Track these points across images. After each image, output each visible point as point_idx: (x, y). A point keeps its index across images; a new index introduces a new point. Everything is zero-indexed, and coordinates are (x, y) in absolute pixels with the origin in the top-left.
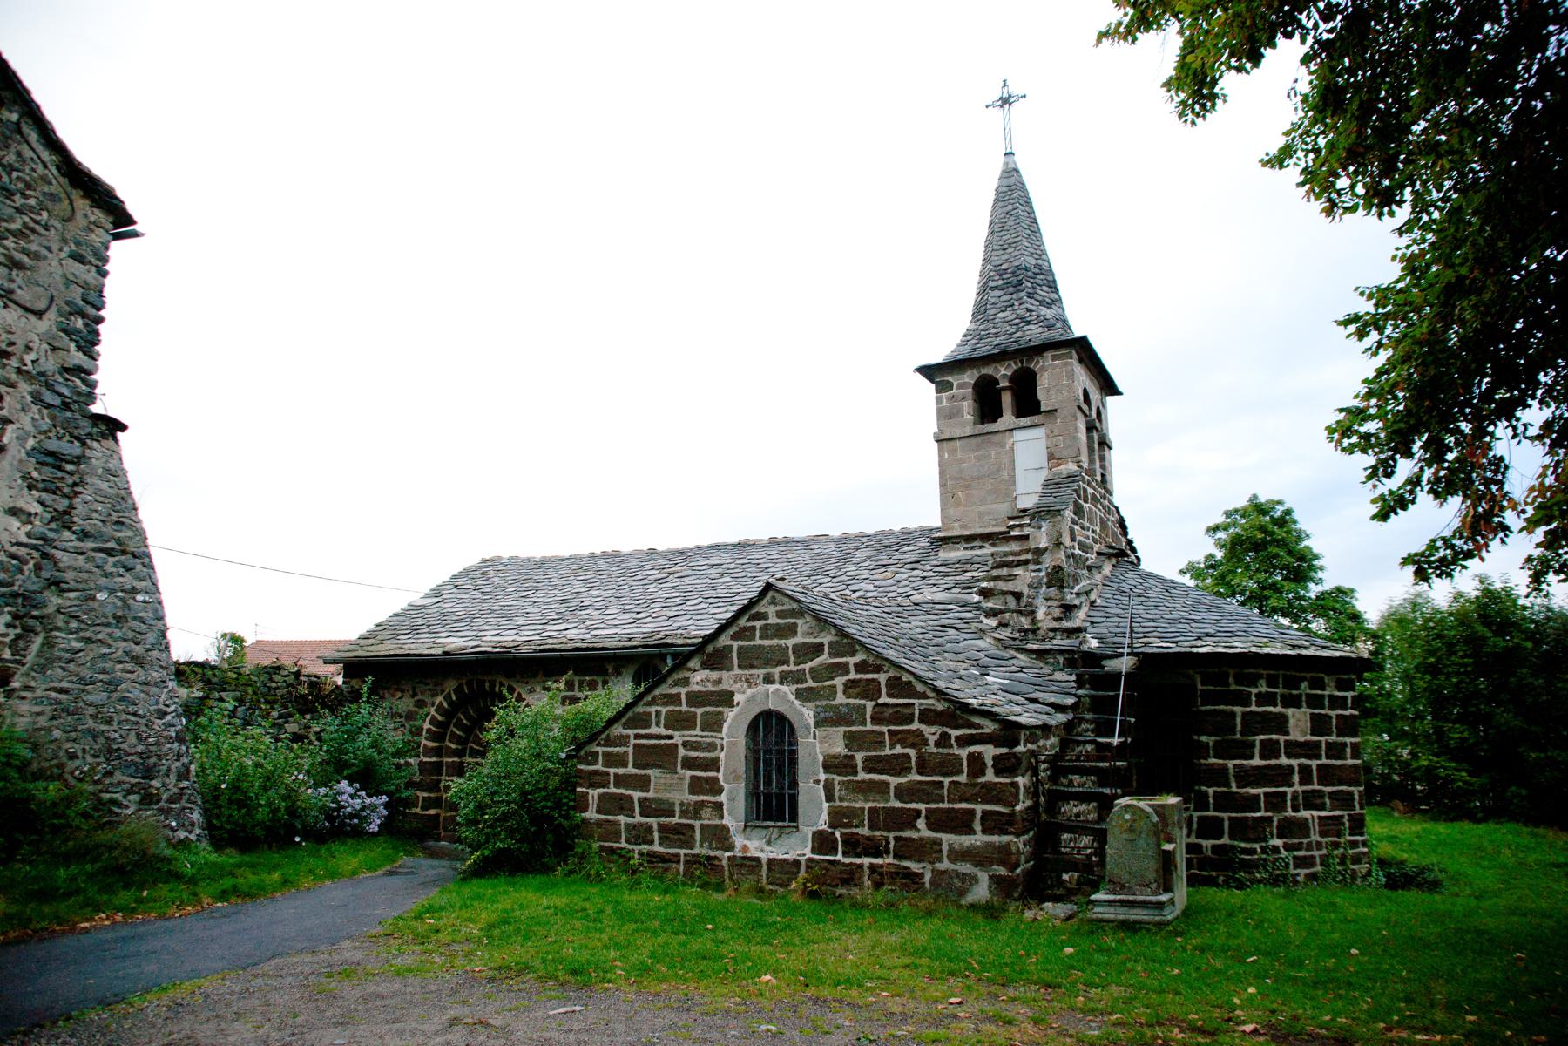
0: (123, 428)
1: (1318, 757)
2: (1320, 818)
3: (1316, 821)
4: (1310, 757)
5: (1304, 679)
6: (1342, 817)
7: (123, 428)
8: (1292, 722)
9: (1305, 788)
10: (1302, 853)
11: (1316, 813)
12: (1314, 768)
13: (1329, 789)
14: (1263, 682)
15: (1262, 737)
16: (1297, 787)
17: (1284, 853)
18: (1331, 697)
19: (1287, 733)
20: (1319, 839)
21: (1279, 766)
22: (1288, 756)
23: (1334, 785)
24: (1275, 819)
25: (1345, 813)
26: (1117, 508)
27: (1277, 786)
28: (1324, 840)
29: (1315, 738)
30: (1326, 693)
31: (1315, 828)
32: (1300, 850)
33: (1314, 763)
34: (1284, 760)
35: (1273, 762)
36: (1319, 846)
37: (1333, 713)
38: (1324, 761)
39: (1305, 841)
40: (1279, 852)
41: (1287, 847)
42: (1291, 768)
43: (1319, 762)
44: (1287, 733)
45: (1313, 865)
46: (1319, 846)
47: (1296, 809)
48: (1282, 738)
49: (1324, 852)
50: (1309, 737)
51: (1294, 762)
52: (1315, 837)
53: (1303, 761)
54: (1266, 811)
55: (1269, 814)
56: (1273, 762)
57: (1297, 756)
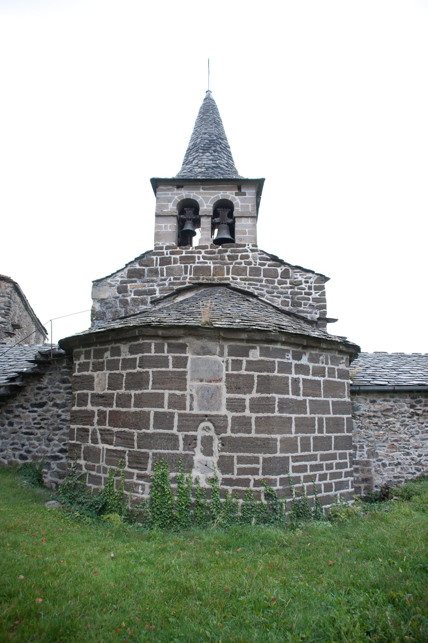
0: (326, 279)
1: (111, 405)
2: (108, 450)
3: (105, 451)
4: (105, 405)
5: (106, 350)
6: (124, 452)
7: (326, 279)
8: (96, 380)
9: (100, 427)
10: (94, 473)
11: (106, 446)
12: (290, 393)
13: (116, 429)
14: (83, 356)
15: (79, 392)
16: (96, 427)
17: (84, 470)
18: (109, 362)
19: (93, 389)
20: (106, 466)
21: (86, 411)
22: (93, 404)
23: (119, 427)
24: (83, 447)
25: (127, 449)
26: (127, 265)
27: (84, 425)
28: (109, 467)
29: (110, 392)
30: (121, 357)
31: (103, 456)
32: (94, 470)
33: (108, 409)
34: (89, 407)
35: (83, 408)
36: (105, 470)
37: (124, 372)
38: (114, 408)
39: (97, 465)
40: (81, 469)
41: (87, 467)
42: (93, 412)
43: (111, 409)
44: (93, 389)
45: (99, 483)
46: (105, 470)
47: (95, 441)
48: (90, 392)
49: (107, 475)
50: (106, 391)
51: (95, 409)
52: (103, 464)
53: (101, 408)
54: (77, 440)
55: (78, 442)
56: (83, 408)
57: (98, 404)
